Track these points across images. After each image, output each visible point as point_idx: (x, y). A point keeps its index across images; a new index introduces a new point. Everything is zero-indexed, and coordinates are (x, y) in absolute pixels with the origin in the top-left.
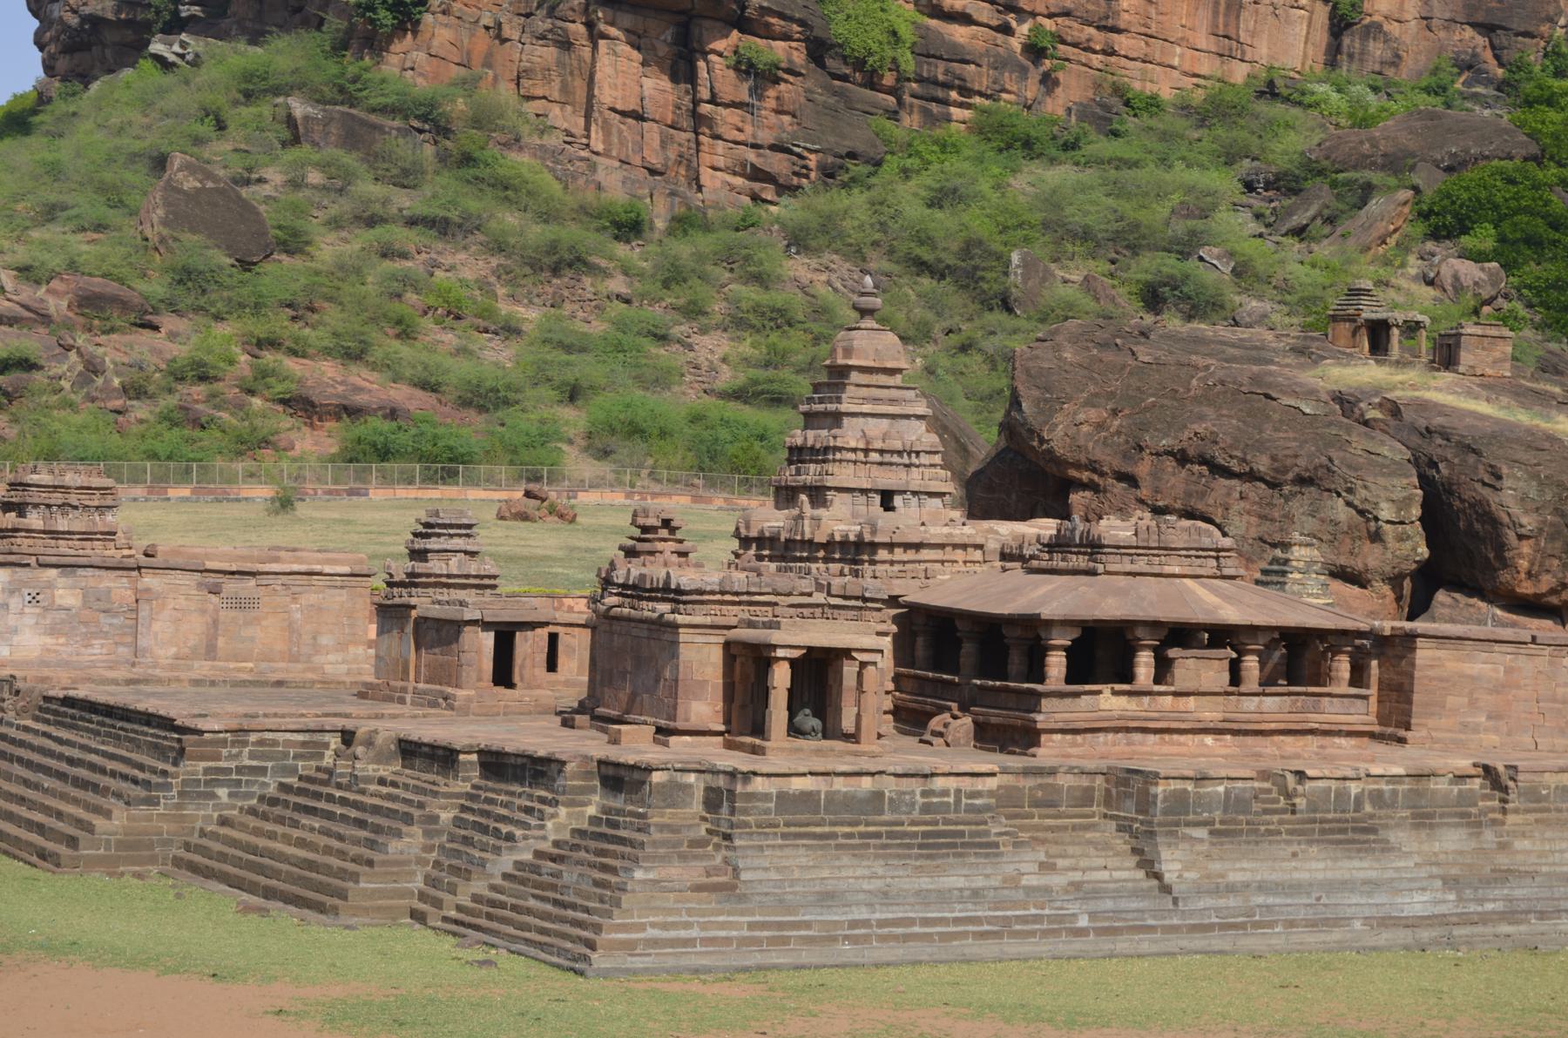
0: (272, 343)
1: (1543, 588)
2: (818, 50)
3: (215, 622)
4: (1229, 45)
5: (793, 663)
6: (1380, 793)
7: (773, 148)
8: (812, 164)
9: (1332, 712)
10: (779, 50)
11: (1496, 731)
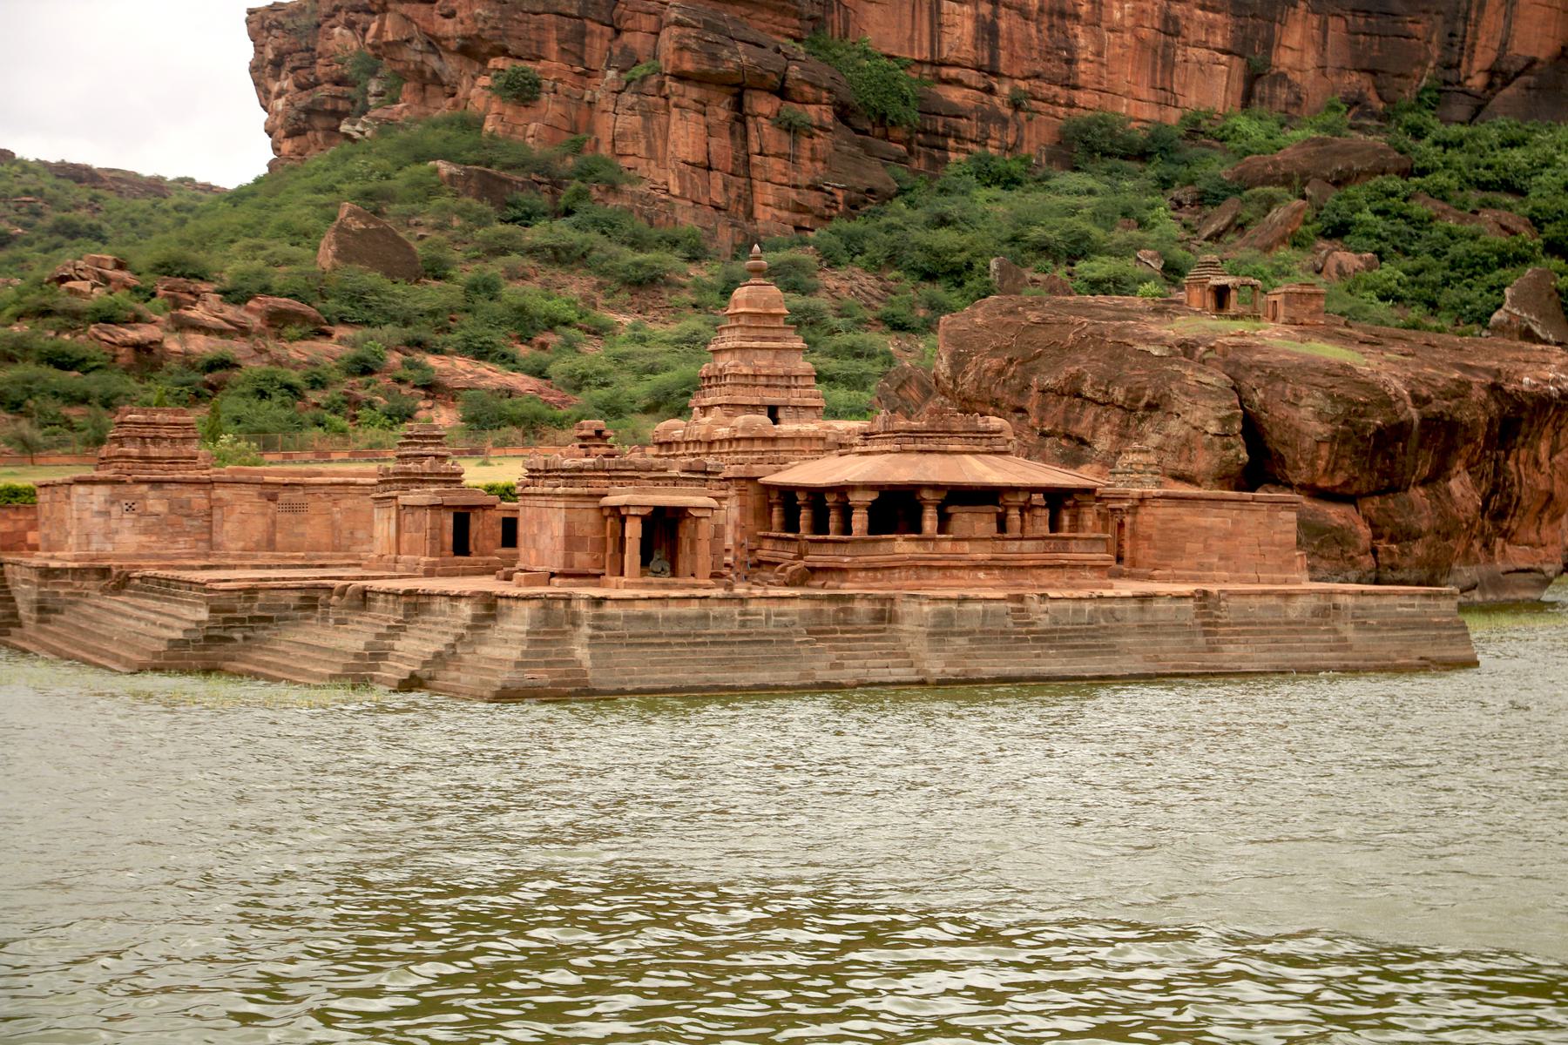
0: (419, 345)
1: (1338, 481)
2: (844, 113)
3: (274, 523)
4: (1166, 96)
5: (644, 519)
6: (1112, 611)
7: (808, 187)
8: (840, 199)
9: (1077, 554)
11: (1227, 569)
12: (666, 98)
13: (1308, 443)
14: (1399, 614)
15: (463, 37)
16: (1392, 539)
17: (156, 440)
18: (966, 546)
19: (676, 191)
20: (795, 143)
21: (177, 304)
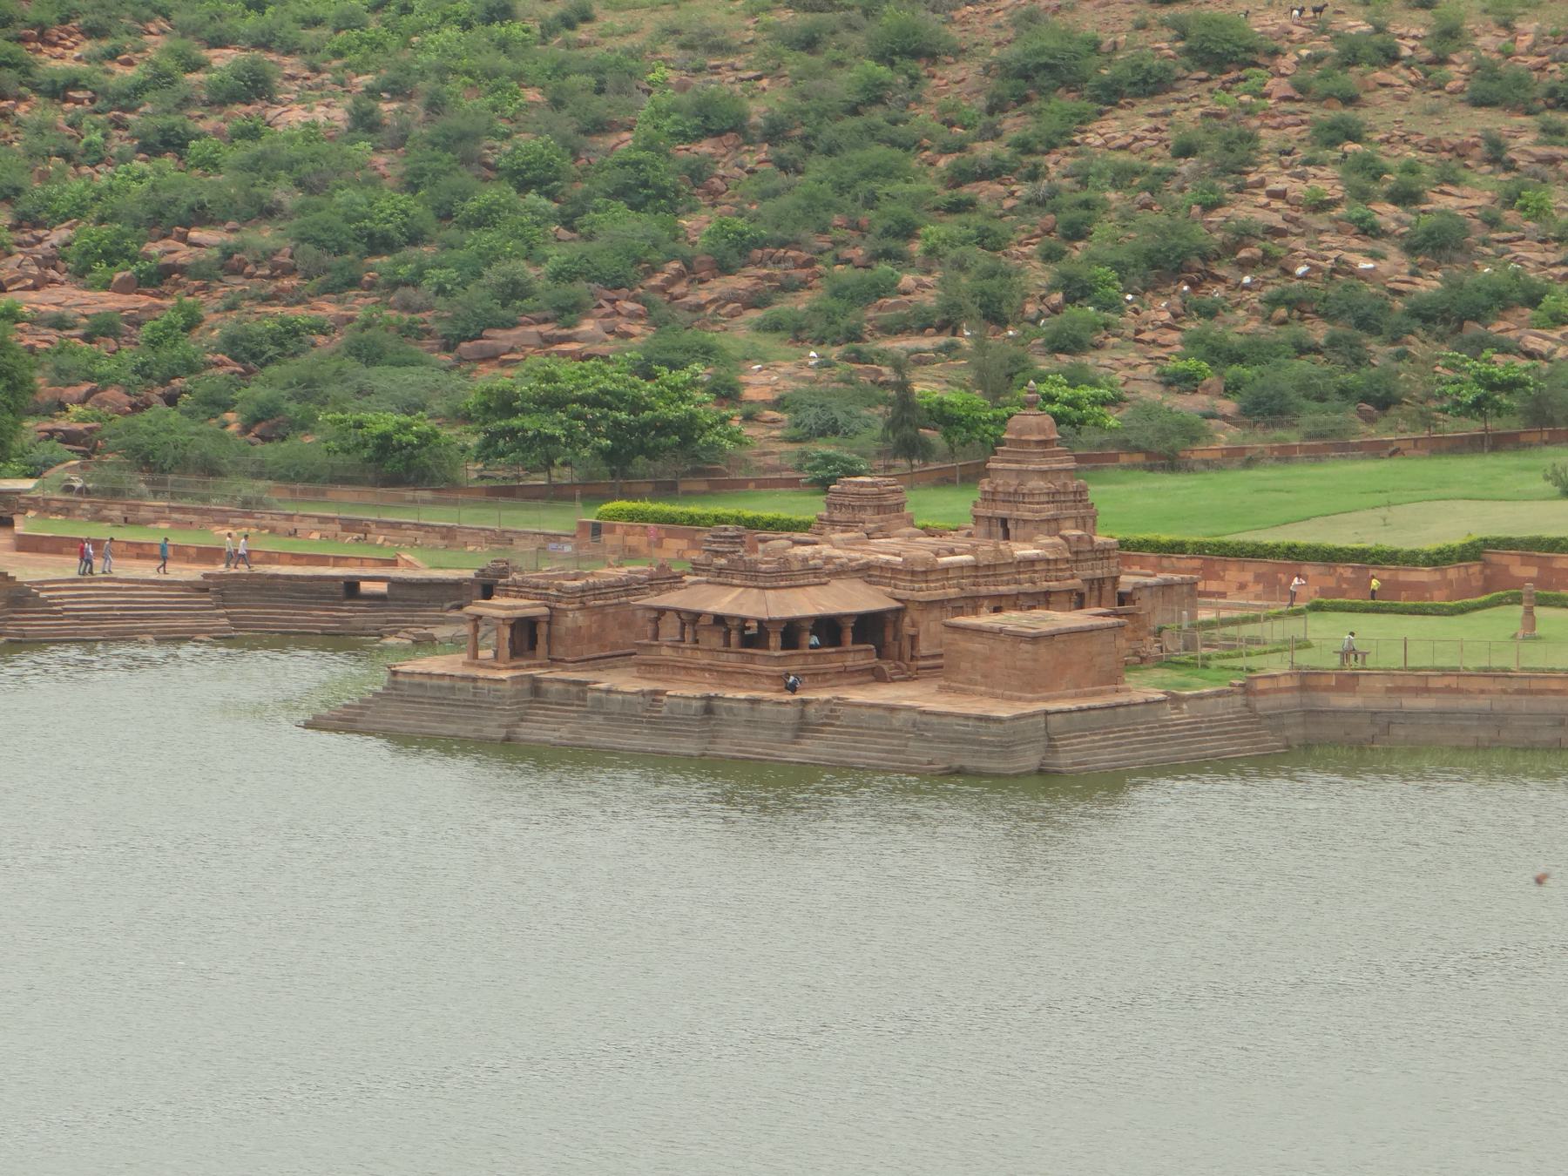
6: (731, 708)
14: (956, 731)
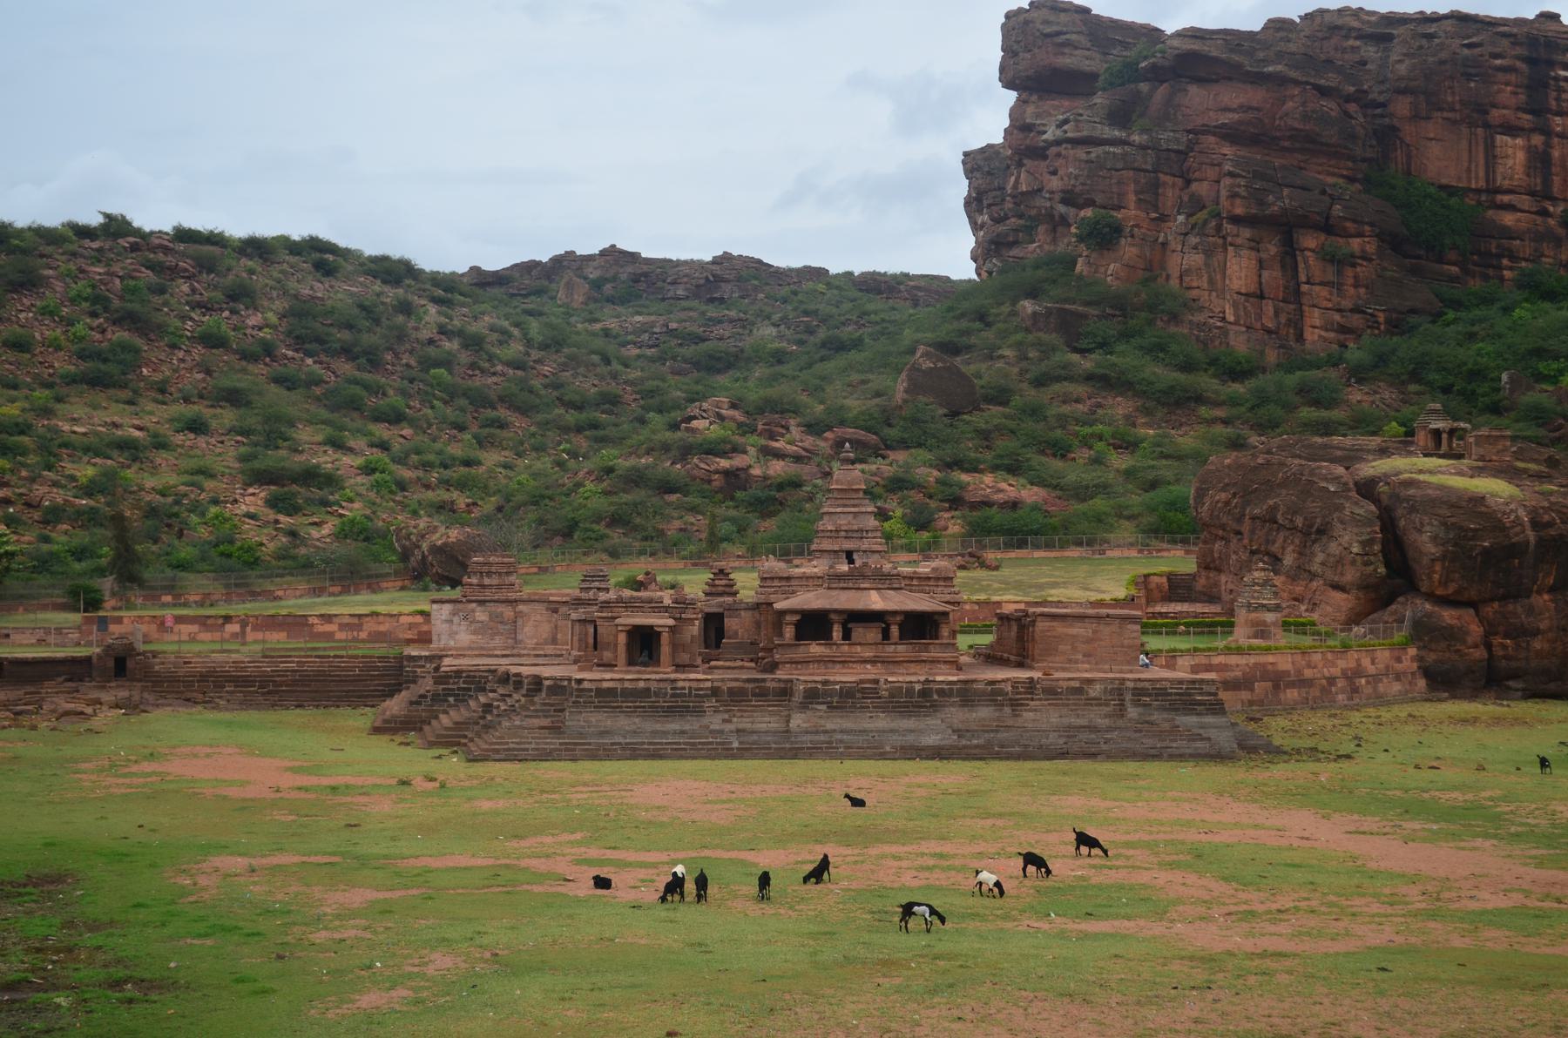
0: (958, 464)
1: (1450, 591)
2: (1393, 243)
5: (628, 632)
7: (1351, 311)
8: (1381, 320)
10: (1356, 243)
12: (1224, 238)
13: (1425, 561)
15: (1063, 191)
16: (1506, 636)
17: (489, 574)
18: (859, 649)
19: (1231, 318)
20: (1340, 273)
21: (772, 437)
